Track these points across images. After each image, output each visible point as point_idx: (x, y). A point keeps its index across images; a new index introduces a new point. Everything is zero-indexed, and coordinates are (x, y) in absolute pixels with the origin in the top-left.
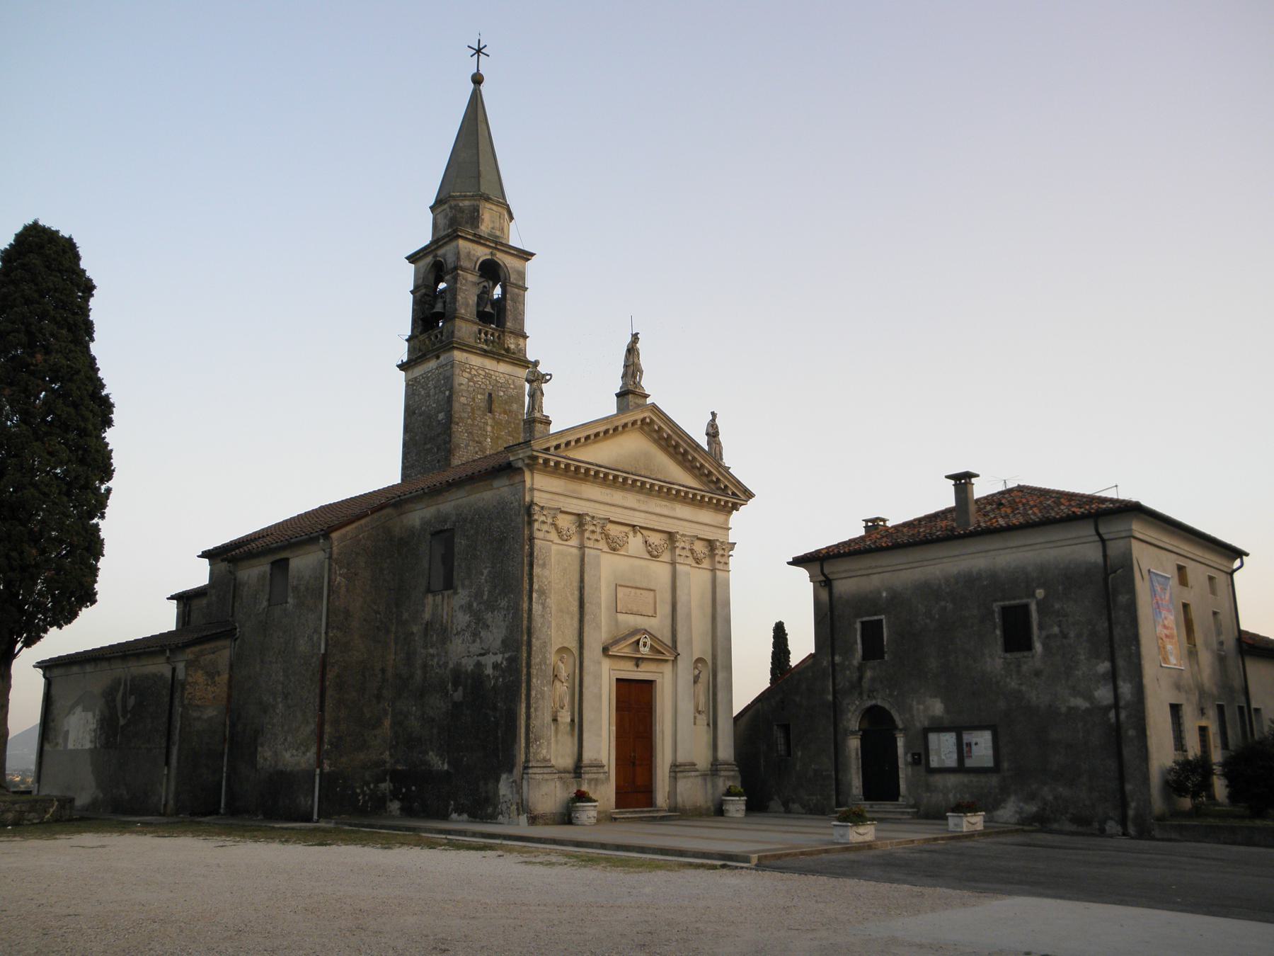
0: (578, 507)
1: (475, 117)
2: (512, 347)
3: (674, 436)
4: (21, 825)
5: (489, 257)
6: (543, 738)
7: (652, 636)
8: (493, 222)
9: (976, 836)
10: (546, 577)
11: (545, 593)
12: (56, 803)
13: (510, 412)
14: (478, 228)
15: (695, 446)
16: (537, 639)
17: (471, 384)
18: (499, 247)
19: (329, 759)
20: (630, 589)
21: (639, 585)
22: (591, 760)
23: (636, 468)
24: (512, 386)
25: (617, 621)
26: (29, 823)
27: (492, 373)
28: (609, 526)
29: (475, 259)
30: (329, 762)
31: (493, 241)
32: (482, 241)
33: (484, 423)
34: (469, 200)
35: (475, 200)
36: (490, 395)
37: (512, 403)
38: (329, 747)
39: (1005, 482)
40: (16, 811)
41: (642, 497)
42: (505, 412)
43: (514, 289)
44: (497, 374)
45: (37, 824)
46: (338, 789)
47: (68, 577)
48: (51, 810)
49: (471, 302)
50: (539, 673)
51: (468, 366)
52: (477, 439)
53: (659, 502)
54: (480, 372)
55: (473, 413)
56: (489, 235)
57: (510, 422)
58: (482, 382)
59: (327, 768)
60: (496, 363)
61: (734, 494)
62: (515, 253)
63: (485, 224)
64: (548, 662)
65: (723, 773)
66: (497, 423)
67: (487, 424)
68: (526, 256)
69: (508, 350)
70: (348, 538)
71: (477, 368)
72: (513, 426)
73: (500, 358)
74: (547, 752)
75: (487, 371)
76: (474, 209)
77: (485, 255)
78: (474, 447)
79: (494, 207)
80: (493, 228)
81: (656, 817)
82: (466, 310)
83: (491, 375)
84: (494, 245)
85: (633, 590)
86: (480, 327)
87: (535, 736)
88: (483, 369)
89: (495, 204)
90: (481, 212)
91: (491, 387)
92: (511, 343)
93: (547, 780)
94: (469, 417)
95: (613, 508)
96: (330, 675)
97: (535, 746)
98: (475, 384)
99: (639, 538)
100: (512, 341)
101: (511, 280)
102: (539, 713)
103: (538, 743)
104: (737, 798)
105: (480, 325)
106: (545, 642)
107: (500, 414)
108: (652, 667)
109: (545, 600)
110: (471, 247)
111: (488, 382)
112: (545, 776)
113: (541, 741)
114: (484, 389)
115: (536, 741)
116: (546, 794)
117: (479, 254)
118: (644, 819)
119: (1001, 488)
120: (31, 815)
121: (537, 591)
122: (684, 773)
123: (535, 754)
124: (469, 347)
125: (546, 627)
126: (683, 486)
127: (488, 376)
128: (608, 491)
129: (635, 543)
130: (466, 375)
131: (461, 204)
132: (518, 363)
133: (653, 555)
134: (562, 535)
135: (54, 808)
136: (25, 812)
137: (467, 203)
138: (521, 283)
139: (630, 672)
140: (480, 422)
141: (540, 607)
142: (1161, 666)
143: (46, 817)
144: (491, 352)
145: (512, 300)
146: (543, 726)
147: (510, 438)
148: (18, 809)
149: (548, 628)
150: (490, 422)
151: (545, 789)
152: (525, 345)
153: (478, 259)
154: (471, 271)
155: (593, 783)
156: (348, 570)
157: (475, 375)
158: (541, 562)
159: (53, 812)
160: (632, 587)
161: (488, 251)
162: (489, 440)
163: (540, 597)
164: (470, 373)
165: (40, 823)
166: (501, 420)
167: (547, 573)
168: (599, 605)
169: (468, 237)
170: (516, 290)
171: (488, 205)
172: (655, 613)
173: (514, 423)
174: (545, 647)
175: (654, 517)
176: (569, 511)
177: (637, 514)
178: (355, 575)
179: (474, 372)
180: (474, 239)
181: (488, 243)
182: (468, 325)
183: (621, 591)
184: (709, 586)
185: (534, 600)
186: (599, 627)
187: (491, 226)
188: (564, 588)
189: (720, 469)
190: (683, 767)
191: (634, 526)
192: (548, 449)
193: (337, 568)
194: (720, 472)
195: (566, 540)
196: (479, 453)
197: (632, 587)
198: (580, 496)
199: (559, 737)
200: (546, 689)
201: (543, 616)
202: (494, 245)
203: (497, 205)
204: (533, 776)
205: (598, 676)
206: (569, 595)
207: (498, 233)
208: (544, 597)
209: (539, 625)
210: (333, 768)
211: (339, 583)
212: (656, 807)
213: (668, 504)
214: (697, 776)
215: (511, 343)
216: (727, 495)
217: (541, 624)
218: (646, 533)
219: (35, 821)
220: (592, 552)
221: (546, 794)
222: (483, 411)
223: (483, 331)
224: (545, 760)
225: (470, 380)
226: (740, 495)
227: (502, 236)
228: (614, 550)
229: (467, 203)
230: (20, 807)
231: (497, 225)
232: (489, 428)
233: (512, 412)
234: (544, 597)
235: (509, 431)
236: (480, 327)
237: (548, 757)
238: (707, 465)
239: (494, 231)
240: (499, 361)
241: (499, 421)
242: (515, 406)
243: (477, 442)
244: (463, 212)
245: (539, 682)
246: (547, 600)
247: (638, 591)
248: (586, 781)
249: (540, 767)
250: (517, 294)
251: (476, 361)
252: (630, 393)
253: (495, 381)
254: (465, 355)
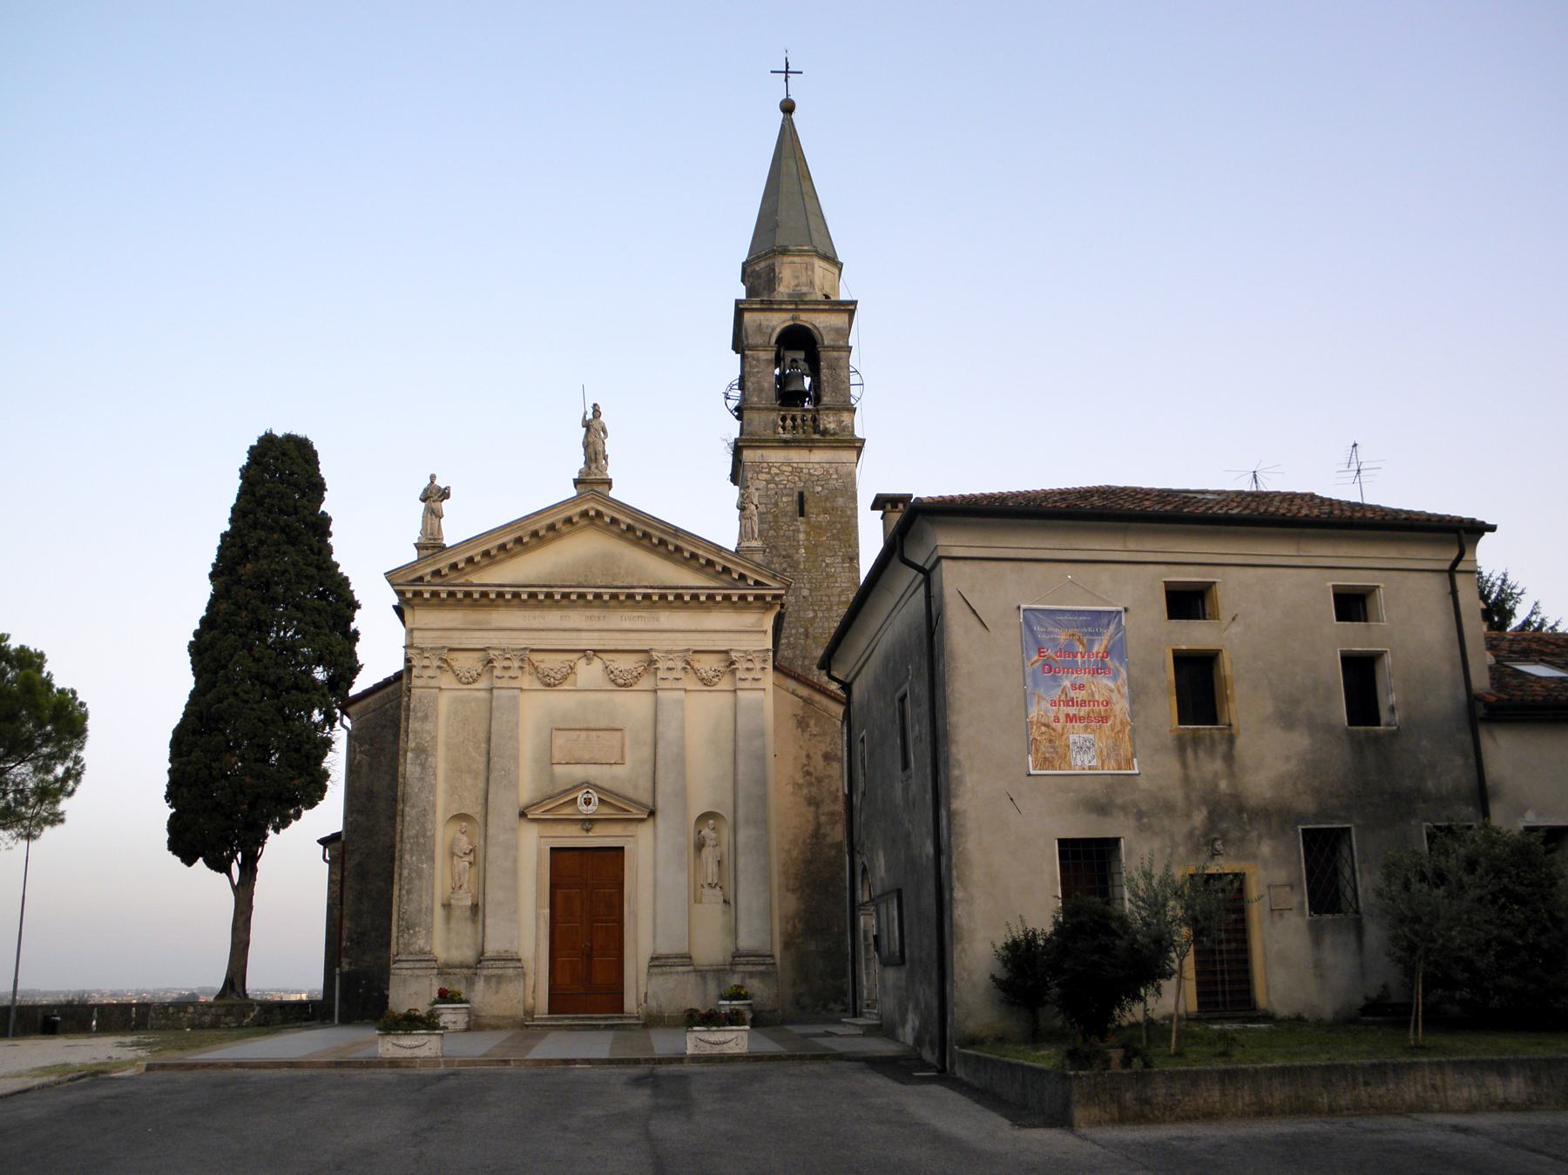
0: (484, 641)
1: (788, 151)
2: (832, 426)
3: (637, 525)
4: (219, 1027)
5: (791, 323)
6: (420, 926)
7: (597, 788)
8: (797, 277)
9: (686, 1061)
10: (428, 732)
11: (426, 750)
12: (258, 1008)
13: (833, 510)
14: (775, 290)
15: (673, 532)
16: (413, 806)
17: (772, 486)
18: (801, 307)
19: (349, 957)
20: (578, 733)
21: (592, 725)
22: (497, 952)
23: (586, 576)
24: (834, 476)
25: (552, 776)
26: (226, 1026)
27: (800, 465)
28: (536, 657)
29: (769, 331)
30: (348, 960)
31: (790, 303)
32: (775, 307)
33: (793, 531)
34: (765, 260)
35: (770, 258)
36: (801, 495)
37: (836, 497)
38: (348, 944)
39: (1255, 476)
40: (213, 1015)
41: (596, 613)
42: (825, 512)
43: (829, 353)
44: (811, 466)
45: (234, 1027)
46: (361, 991)
47: (267, 781)
48: (252, 1015)
49: (766, 385)
50: (414, 849)
51: (765, 465)
52: (784, 553)
53: (627, 614)
54: (784, 468)
55: (776, 522)
56: (790, 295)
57: (834, 523)
58: (788, 481)
59: (346, 967)
60: (808, 452)
61: (757, 583)
62: (827, 307)
63: (785, 283)
64: (429, 834)
65: (740, 968)
66: (816, 528)
67: (799, 531)
68: (849, 308)
69: (825, 432)
70: (370, 710)
71: (779, 464)
72: (839, 526)
73: (809, 445)
74: (426, 942)
75: (795, 465)
76: (770, 269)
77: (784, 322)
78: (781, 564)
79: (796, 259)
80: (797, 286)
81: (600, 1025)
82: (759, 396)
83: (802, 469)
84: (793, 307)
85: (583, 734)
86: (782, 413)
87: (407, 923)
88: (789, 464)
89: (797, 255)
90: (777, 270)
91: (802, 484)
92: (830, 423)
93: (418, 976)
94: (771, 528)
95: (543, 633)
96: (350, 864)
97: (406, 936)
98: (777, 485)
99: (597, 664)
100: (831, 419)
101: (826, 343)
102: (414, 896)
103: (411, 932)
104: (728, 1002)
105: (780, 410)
106: (425, 810)
107: (818, 515)
108: (617, 829)
109: (426, 759)
110: (762, 318)
111: (797, 479)
112: (416, 971)
113: (417, 929)
114: (792, 489)
115: (409, 929)
116: (416, 993)
117: (775, 323)
118: (577, 1028)
119: (1246, 486)
120: (228, 1019)
121: (412, 750)
122: (664, 968)
123: (407, 945)
124: (760, 442)
125: (427, 792)
126: (651, 587)
127: (796, 471)
128: (537, 613)
129: (589, 673)
130: (764, 476)
131: (757, 269)
132: (839, 445)
133: (622, 683)
134: (461, 678)
135: (256, 1012)
136: (221, 1015)
137: (763, 264)
138: (841, 343)
139: (572, 837)
140: (789, 530)
141: (418, 769)
142: (1029, 775)
143: (246, 1021)
144: (794, 441)
145: (831, 367)
146: (420, 911)
147: (835, 542)
148: (214, 1012)
149: (430, 792)
150: (802, 528)
151: (414, 986)
152: (853, 420)
153: (774, 329)
154: (765, 348)
155: (494, 981)
156: (372, 745)
157: (777, 474)
158: (419, 715)
159: (255, 1016)
160: (580, 730)
161: (788, 316)
162: (803, 551)
163: (417, 757)
164: (769, 473)
165: (238, 1027)
166: (820, 522)
167: (428, 726)
168: (516, 758)
169: (754, 306)
170: (835, 353)
171: (786, 259)
172: (623, 757)
173: (840, 523)
174: (424, 815)
175: (618, 635)
176: (470, 647)
177: (584, 635)
178: (381, 750)
179: (774, 470)
180: (763, 306)
181: (784, 307)
182: (762, 414)
183: (560, 739)
184: (729, 714)
185: (408, 761)
186: (514, 786)
187: (793, 283)
188: (463, 742)
189: (723, 554)
190: (663, 960)
191: (584, 651)
192: (421, 579)
193: (357, 746)
194: (723, 558)
195: (468, 683)
196: (788, 570)
197: (580, 730)
198: (489, 627)
199: (453, 924)
200: (425, 866)
201: (423, 779)
202: (793, 307)
203: (800, 255)
204: (398, 971)
205: (512, 848)
206: (471, 749)
207: (804, 289)
208: (424, 756)
209: (417, 790)
210: (353, 967)
211: (359, 762)
212: (623, 1013)
213: (643, 614)
214: (688, 972)
215: (829, 422)
216: (749, 587)
217: (419, 789)
218: (605, 656)
219: (233, 1025)
220: (504, 692)
221: (416, 993)
222: (791, 517)
223: (789, 418)
224: (422, 952)
225: (768, 482)
226: (770, 583)
227: (811, 291)
228: (549, 685)
229: (763, 264)
230: (216, 1011)
231: (803, 279)
232: (802, 536)
233: (837, 508)
234: (424, 756)
235: (833, 535)
236: (782, 413)
237: (428, 949)
238: (700, 552)
239: (799, 288)
240: (810, 449)
241: (817, 524)
242: (840, 501)
243: (784, 557)
244: (760, 276)
245: (414, 858)
246: (430, 759)
247: (593, 734)
248: (482, 978)
249: (413, 961)
250: (836, 359)
251: (775, 456)
252: (592, 481)
253: (807, 476)
254: (759, 452)
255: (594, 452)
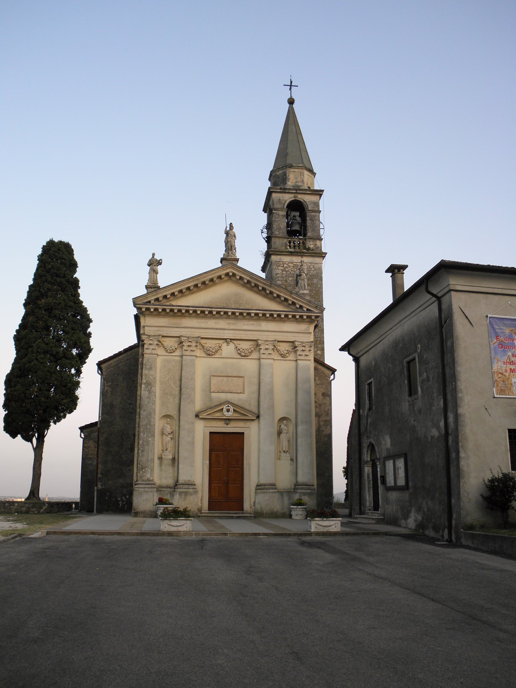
0: (179, 333)
2: (312, 246)
3: (252, 281)
4: (29, 513)
5: (294, 199)
7: (233, 404)
8: (297, 178)
9: (313, 535)
10: (152, 375)
12: (47, 505)
14: (286, 184)
15: (269, 284)
16: (145, 411)
17: (284, 272)
18: (298, 192)
19: (101, 482)
20: (222, 378)
21: (230, 375)
22: (185, 481)
25: (211, 399)
26: (32, 513)
27: (297, 264)
28: (203, 341)
29: (284, 202)
31: (294, 190)
32: (287, 191)
34: (281, 170)
35: (284, 169)
37: (313, 278)
38: (101, 476)
41: (231, 321)
43: (311, 213)
46: (107, 498)
48: (44, 508)
49: (282, 226)
51: (281, 263)
53: (246, 322)
54: (290, 265)
56: (293, 186)
58: (292, 270)
59: (100, 487)
61: (308, 310)
62: (310, 192)
63: (290, 181)
64: (152, 424)
65: (299, 491)
68: (319, 193)
69: (309, 249)
71: (288, 263)
72: (314, 292)
73: (302, 254)
74: (151, 475)
75: (295, 263)
76: (284, 174)
77: (291, 198)
79: (296, 170)
80: (296, 182)
81: (233, 517)
84: (295, 191)
85: (225, 378)
87: (142, 466)
88: (292, 263)
90: (287, 175)
92: (311, 245)
93: (147, 491)
98: (287, 272)
99: (232, 346)
101: (309, 208)
103: (144, 470)
104: (296, 507)
105: (288, 238)
106: (150, 412)
108: (241, 424)
109: (151, 388)
110: (281, 196)
111: (296, 270)
112: (146, 489)
113: (146, 469)
115: (142, 469)
117: (286, 199)
121: (145, 384)
124: (280, 252)
126: (259, 310)
128: (204, 320)
129: (228, 349)
131: (278, 174)
134: (167, 350)
136: (31, 508)
137: (280, 172)
138: (316, 209)
139: (220, 427)
141: (147, 393)
142: (494, 397)
143: (41, 510)
144: (295, 252)
146: (148, 460)
148: (27, 506)
149: (153, 404)
151: (145, 497)
152: (321, 244)
153: (286, 201)
154: (282, 209)
155: (183, 494)
156: (112, 383)
158: (148, 367)
160: (224, 376)
163: (147, 387)
164: (283, 266)
165: (38, 513)
167: (152, 372)
168: (194, 389)
169: (277, 191)
170: (313, 213)
171: (292, 170)
172: (244, 390)
173: (315, 290)
174: (150, 415)
177: (226, 331)
179: (285, 266)
180: (281, 191)
181: (291, 191)
183: (214, 380)
184: (294, 371)
185: (142, 388)
186: (193, 402)
187: (294, 181)
188: (168, 381)
191: (226, 339)
192: (149, 302)
194: (293, 298)
195: (171, 353)
198: (181, 326)
199: (163, 467)
200: (150, 439)
201: (149, 397)
202: (295, 191)
205: (192, 432)
206: (172, 384)
207: (300, 184)
208: (150, 387)
209: (146, 403)
210: (103, 487)
211: (107, 391)
213: (254, 323)
214: (275, 492)
215: (310, 244)
216: (304, 312)
217: (147, 402)
218: (235, 342)
219: (35, 512)
224: (149, 480)
225: (283, 271)
227: (302, 185)
228: (209, 355)
229: (280, 172)
231: (299, 179)
233: (314, 284)
234: (150, 387)
237: (151, 479)
238: (282, 294)
239: (297, 183)
240: (302, 256)
242: (315, 281)
245: (145, 435)
246: (152, 388)
247: (230, 378)
248: (178, 493)
250: (314, 216)
251: (286, 259)
254: (279, 257)
255: (230, 247)
